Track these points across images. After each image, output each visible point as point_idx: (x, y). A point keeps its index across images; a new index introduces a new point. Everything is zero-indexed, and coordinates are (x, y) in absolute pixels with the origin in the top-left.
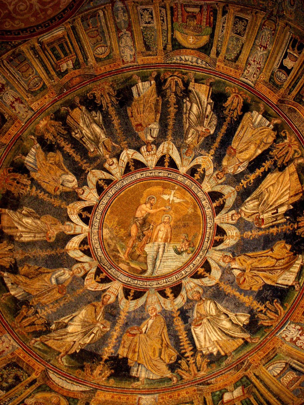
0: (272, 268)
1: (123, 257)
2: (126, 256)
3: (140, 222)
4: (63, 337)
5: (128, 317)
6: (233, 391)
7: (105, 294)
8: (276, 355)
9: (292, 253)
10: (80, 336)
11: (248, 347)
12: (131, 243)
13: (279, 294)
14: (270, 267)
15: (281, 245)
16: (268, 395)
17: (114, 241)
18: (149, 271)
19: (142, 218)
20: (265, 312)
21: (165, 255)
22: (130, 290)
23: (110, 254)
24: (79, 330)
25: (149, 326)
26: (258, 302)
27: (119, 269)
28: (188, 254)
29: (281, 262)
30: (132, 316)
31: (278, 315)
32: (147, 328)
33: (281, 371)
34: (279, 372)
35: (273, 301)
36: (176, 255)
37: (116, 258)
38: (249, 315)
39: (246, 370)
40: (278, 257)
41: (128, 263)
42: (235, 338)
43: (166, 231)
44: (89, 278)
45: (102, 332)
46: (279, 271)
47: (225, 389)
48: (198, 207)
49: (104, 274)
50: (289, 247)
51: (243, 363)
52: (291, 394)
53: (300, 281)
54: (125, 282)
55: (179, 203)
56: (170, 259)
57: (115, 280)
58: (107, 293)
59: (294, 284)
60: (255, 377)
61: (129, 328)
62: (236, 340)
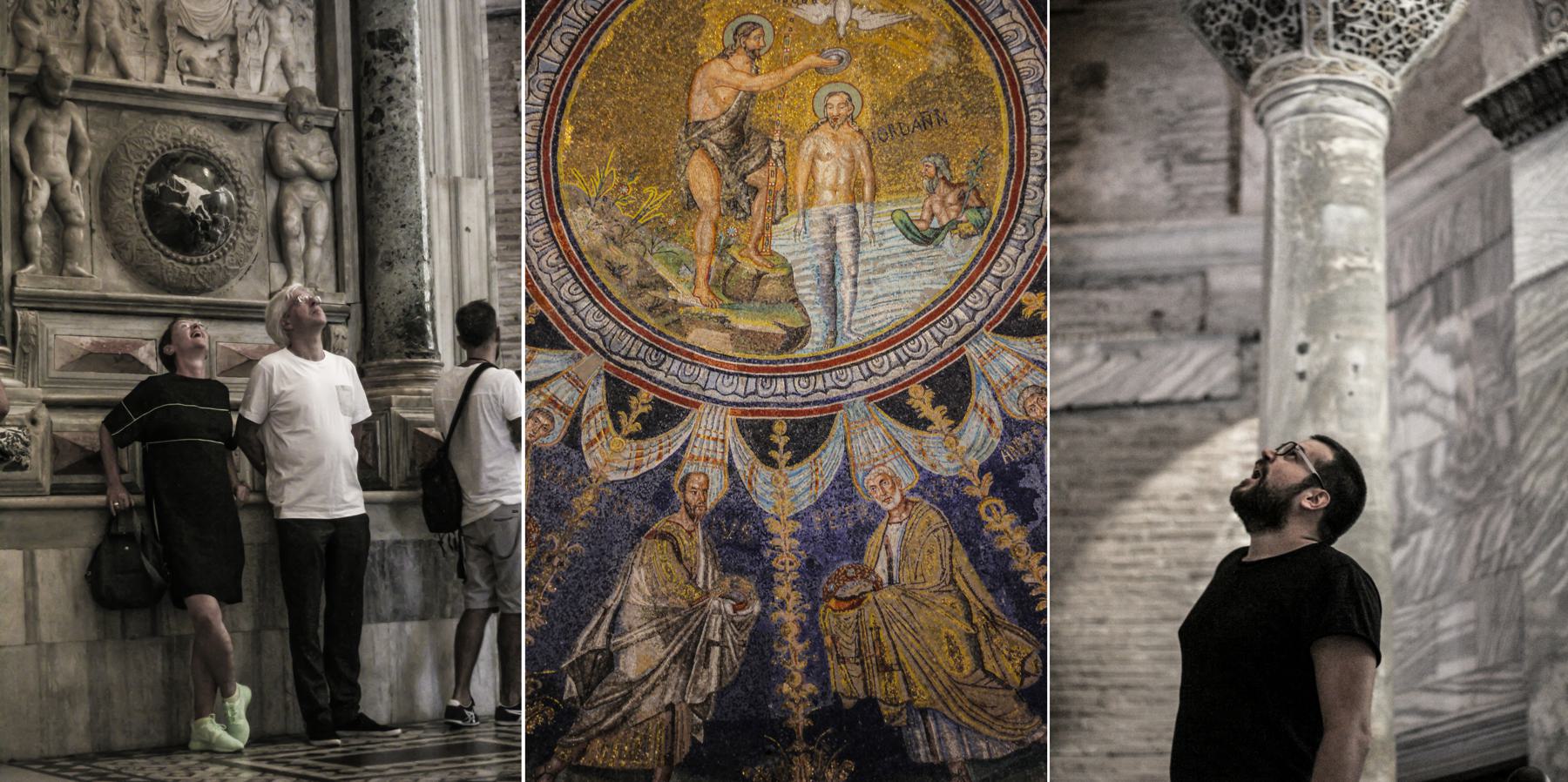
1: (692, 301)
2: (703, 291)
3: (723, 137)
4: (625, 708)
5: (806, 539)
7: (680, 475)
10: (676, 678)
12: (704, 234)
17: (633, 247)
18: (818, 329)
19: (724, 120)
21: (868, 251)
22: (771, 423)
23: (637, 306)
24: (662, 655)
25: (894, 550)
27: (691, 355)
28: (969, 236)
30: (818, 529)
32: (890, 561)
36: (915, 247)
37: (666, 312)
41: (723, 320)
43: (847, 155)
44: (594, 435)
45: (739, 625)
48: (976, 40)
49: (644, 393)
54: (739, 399)
55: (886, 30)
56: (893, 266)
57: (697, 406)
58: (687, 467)
61: (825, 579)
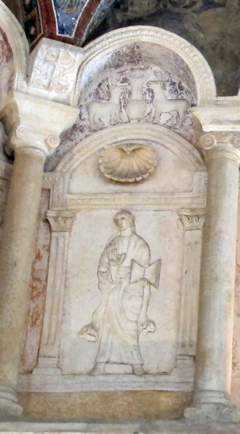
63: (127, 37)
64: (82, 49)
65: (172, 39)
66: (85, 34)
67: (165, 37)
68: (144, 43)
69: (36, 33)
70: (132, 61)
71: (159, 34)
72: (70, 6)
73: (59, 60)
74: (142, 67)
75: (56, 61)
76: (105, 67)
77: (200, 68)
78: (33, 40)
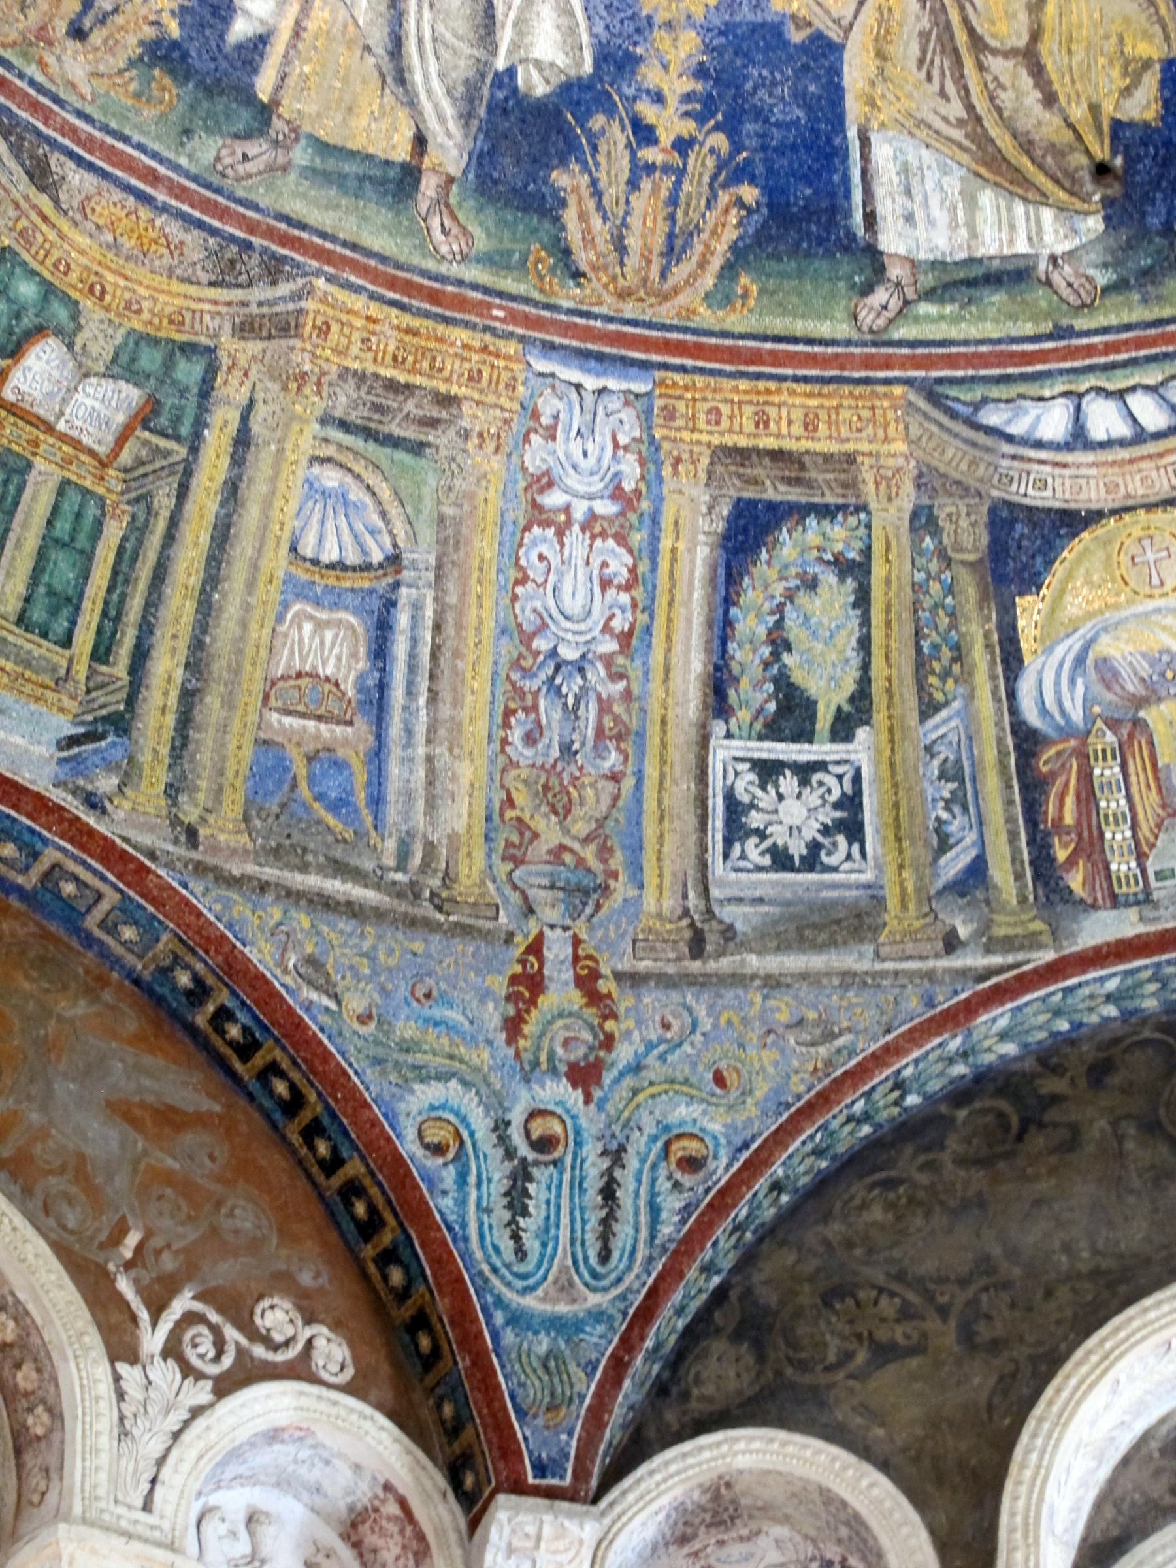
0: (961, 38)
6: (86, 375)
8: (417, 449)
9: (1101, 152)
11: (385, 216)
13: (803, 203)
14: (966, 21)
15: (1147, 36)
16: (179, 608)
20: (650, 168)
26: (701, 72)
29: (1019, 95)
31: (663, 275)
33: (339, 566)
34: (330, 554)
35: (742, 173)
38: (588, 68)
39: (247, 329)
40: (1043, 48)
42: (398, 74)
46: (956, 109)
47: (74, 308)
50: (1143, 105)
51: (274, 269)
52: (248, 752)
53: (926, 308)
59: (895, 272)
60: (233, 417)
62: (388, 98)
63: (700, 1464)
64: (594, 1509)
65: (808, 1453)
66: (596, 1471)
67: (790, 1449)
68: (741, 1472)
69: (478, 1485)
70: (717, 1523)
71: (776, 1446)
72: (552, 1408)
73: (543, 1545)
74: (745, 1532)
75: (537, 1546)
76: (654, 1549)
77: (891, 1513)
78: (474, 1508)
